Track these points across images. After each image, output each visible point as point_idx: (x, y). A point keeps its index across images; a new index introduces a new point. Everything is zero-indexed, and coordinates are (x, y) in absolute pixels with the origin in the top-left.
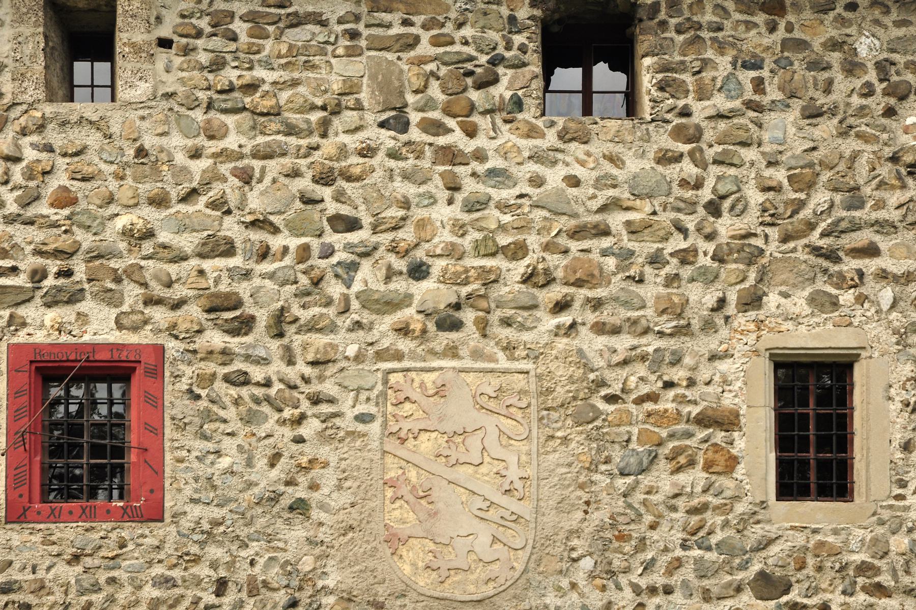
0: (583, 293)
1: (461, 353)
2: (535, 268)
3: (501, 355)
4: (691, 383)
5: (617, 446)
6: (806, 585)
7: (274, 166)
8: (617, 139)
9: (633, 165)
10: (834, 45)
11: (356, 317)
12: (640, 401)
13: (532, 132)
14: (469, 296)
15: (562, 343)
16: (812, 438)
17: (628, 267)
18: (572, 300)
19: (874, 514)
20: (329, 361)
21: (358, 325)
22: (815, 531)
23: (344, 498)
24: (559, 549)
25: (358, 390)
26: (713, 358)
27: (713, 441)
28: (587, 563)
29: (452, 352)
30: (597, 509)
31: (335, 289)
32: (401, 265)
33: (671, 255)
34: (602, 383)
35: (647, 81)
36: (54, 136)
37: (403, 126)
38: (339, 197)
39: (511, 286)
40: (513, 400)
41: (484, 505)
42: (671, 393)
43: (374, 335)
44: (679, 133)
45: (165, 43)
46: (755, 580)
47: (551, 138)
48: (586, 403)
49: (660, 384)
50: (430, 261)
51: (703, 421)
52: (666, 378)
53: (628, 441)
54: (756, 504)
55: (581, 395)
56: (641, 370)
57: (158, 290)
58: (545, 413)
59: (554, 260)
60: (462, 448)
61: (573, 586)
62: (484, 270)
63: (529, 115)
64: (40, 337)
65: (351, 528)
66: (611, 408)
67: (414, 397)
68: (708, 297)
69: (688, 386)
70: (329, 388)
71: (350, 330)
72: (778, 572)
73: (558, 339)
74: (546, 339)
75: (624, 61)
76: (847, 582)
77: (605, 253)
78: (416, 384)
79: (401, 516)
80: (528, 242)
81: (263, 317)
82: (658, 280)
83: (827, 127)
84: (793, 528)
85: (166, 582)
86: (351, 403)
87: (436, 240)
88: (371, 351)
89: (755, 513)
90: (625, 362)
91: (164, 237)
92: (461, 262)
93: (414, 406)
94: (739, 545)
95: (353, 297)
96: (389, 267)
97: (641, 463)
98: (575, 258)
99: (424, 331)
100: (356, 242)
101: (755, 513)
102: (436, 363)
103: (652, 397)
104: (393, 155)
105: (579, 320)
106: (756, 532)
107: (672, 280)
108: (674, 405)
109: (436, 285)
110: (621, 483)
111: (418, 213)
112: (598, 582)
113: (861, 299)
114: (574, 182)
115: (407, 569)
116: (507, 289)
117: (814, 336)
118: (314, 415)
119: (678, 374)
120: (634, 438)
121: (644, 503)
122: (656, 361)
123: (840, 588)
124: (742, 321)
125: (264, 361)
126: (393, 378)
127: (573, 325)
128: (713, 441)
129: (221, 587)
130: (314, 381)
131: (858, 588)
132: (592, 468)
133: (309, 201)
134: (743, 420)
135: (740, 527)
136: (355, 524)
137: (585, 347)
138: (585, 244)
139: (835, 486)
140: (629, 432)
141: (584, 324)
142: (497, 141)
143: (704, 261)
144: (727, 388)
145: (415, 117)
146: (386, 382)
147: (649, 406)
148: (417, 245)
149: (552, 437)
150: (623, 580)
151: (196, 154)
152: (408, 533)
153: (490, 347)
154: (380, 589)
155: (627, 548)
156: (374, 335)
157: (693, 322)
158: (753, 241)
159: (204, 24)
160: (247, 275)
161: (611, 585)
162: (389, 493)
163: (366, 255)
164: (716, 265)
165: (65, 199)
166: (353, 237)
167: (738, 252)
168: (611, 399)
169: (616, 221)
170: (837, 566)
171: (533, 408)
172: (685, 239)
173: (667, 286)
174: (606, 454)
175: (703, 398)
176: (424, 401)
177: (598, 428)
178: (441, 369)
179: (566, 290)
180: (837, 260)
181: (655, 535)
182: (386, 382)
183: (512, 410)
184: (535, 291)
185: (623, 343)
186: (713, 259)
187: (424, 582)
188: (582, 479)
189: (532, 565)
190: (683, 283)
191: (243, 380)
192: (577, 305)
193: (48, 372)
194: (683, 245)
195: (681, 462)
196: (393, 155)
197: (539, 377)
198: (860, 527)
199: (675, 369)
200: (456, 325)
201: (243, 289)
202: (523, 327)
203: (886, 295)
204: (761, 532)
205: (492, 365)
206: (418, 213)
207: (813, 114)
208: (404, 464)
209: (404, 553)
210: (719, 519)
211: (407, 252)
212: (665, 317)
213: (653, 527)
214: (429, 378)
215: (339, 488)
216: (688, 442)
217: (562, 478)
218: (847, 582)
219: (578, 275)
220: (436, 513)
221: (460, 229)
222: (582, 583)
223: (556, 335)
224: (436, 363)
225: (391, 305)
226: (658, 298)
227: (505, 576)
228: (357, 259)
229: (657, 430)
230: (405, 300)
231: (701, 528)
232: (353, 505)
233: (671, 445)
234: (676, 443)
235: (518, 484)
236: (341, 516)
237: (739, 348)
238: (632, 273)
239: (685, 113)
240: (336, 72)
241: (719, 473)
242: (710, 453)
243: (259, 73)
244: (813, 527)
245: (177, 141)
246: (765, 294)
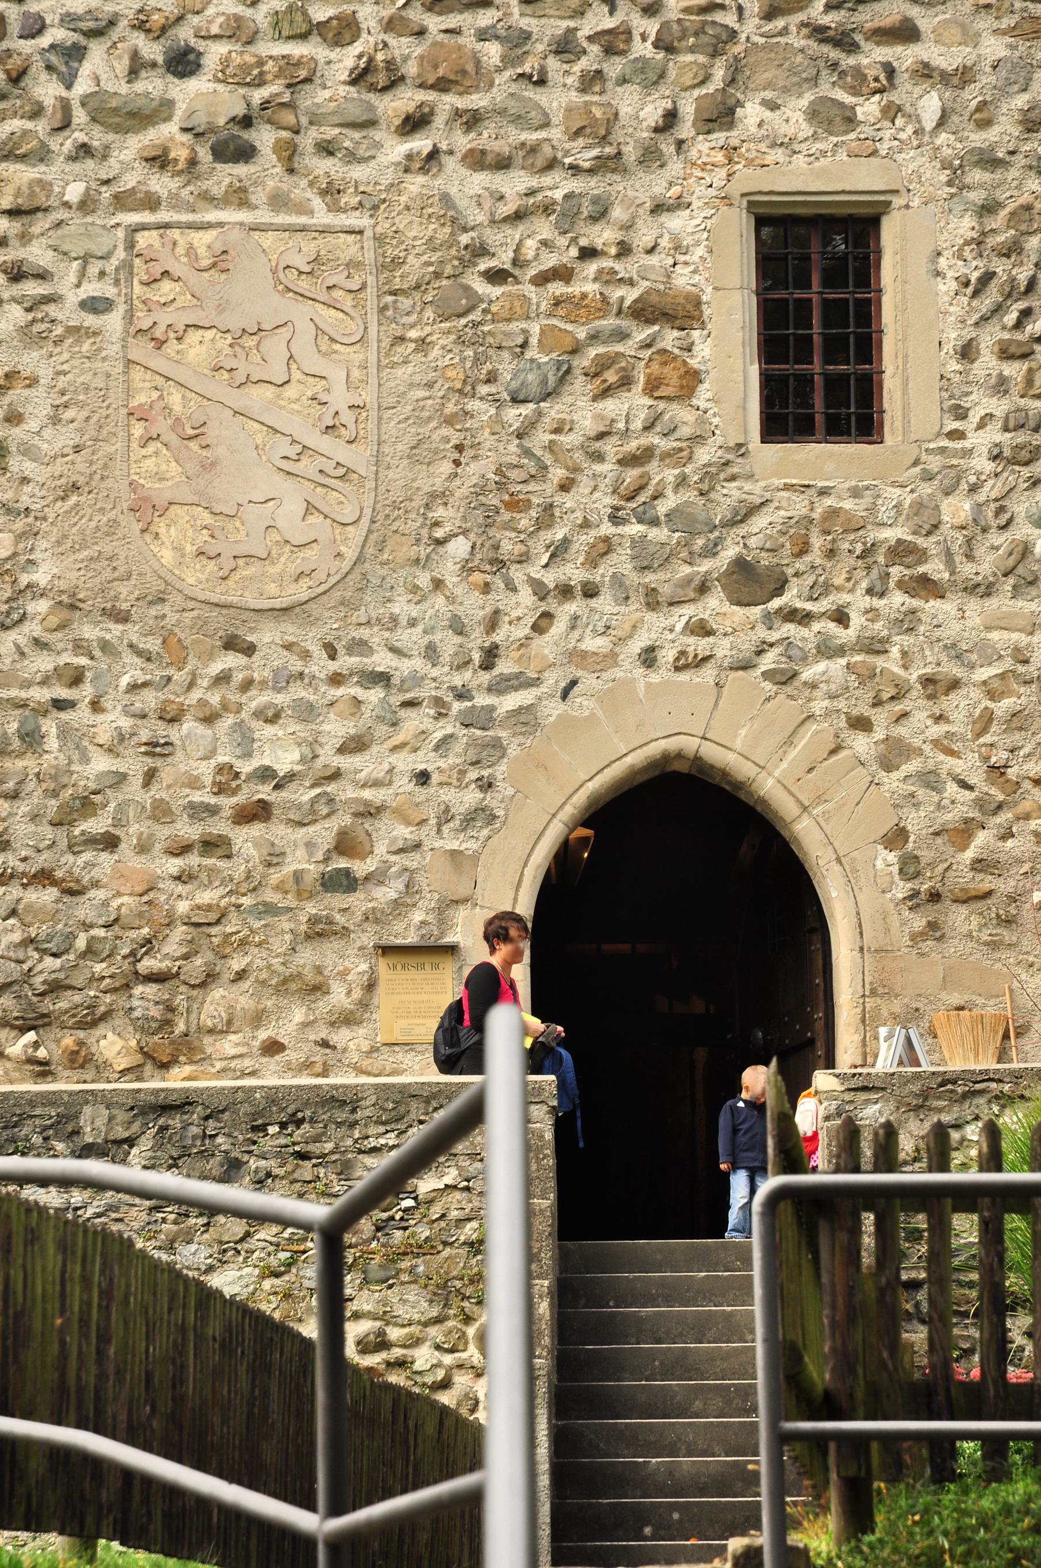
0: (450, 101)
1: (253, 199)
2: (371, 60)
3: (317, 203)
4: (624, 250)
5: (506, 355)
6: (810, 580)
11: (81, 137)
12: (542, 279)
14: (265, 105)
15: (415, 184)
16: (817, 340)
17: (520, 60)
18: (432, 113)
19: (916, 463)
20: (37, 210)
21: (84, 150)
22: (823, 492)
23: (63, 438)
24: (414, 524)
25: (86, 259)
26: (658, 208)
27: (660, 345)
28: (459, 547)
29: (239, 196)
30: (475, 457)
32: (153, 51)
33: (590, 39)
34: (481, 251)
40: (339, 278)
41: (292, 451)
42: (592, 268)
43: (111, 167)
46: (729, 573)
49: (574, 252)
50: (201, 45)
51: (644, 312)
52: (583, 242)
53: (524, 345)
54: (728, 449)
55: (448, 270)
56: (544, 228)
58: (389, 299)
59: (401, 46)
60: (255, 357)
61: (438, 584)
62: (289, 63)
65: (75, 487)
66: (496, 291)
67: (176, 270)
68: (649, 108)
69: (618, 256)
70: (38, 254)
71: (73, 158)
72: (766, 560)
73: (409, 177)
74: (389, 177)
76: (875, 573)
77: (483, 35)
78: (180, 250)
79: (157, 468)
80: (360, 16)
82: (569, 80)
84: (788, 487)
86: (73, 279)
87: (211, 11)
88: (106, 193)
89: (727, 463)
90: (518, 216)
92: (251, 49)
93: (177, 287)
94: (702, 516)
95: (75, 104)
96: (135, 55)
97: (544, 382)
98: (435, 44)
99: (193, 162)
100: (80, 11)
101: (727, 463)
102: (212, 216)
103: (562, 274)
105: (444, 146)
106: (729, 495)
108: (596, 286)
109: (211, 85)
110: (515, 415)
112: (478, 577)
113: (891, 112)
115: (167, 556)
116: (327, 94)
117: (820, 174)
118: (14, 300)
119: (603, 236)
120: (534, 341)
121: (551, 447)
122: (568, 214)
123: (864, 585)
124: (703, 148)
126: (143, 239)
127: (434, 155)
128: (660, 345)
130: (13, 242)
131: (892, 585)
132: (466, 390)
134: (707, 311)
135: (705, 487)
136: (81, 481)
137: (453, 191)
138: (452, 21)
139: (853, 418)
140: (524, 331)
141: (451, 153)
143: (641, 49)
144: (681, 258)
146: (130, 245)
147: (557, 288)
148: (180, 19)
149: (402, 339)
150: (517, 574)
152: (168, 496)
153: (300, 189)
154: (123, 589)
155: (524, 522)
156: (111, 167)
157: (626, 149)
158: (719, 17)
161: (499, 582)
162: (138, 430)
163: (97, 33)
164: (661, 55)
167: (696, 34)
168: (497, 276)
170: (859, 548)
171: (371, 292)
172: (611, 13)
173: (583, 91)
174: (488, 366)
176: (193, 278)
177: (475, 325)
178: (221, 224)
179: (422, 96)
180: (853, 48)
181: (568, 501)
182: (130, 245)
183: (337, 294)
184: (372, 97)
185: (514, 184)
186: (656, 45)
187: (195, 577)
188: (450, 408)
189: (370, 550)
190: (609, 85)
192: (439, 120)
194: (609, 23)
197: (379, 240)
198: (893, 484)
199: (597, 227)
200: (245, 153)
202: (352, 157)
204: (736, 494)
205: (303, 220)
208: (160, 381)
209: (162, 530)
210: (671, 474)
211: (164, 30)
212: (581, 142)
213: (565, 487)
214: (202, 239)
215: (55, 420)
216: (619, 348)
217: (419, 405)
218: (875, 573)
219: (441, 72)
220: (213, 464)
222: (451, 580)
223: (407, 170)
224: (212, 216)
226: (569, 110)
227: (327, 568)
228: (83, 41)
229: (569, 327)
230: (163, 110)
231: (642, 488)
232: (77, 449)
233: (592, 352)
234: (601, 350)
235: (347, 417)
236: (58, 467)
237: (699, 194)
238: (527, 68)
241: (669, 399)
242: (655, 366)
244: (820, 484)
246: (739, 104)
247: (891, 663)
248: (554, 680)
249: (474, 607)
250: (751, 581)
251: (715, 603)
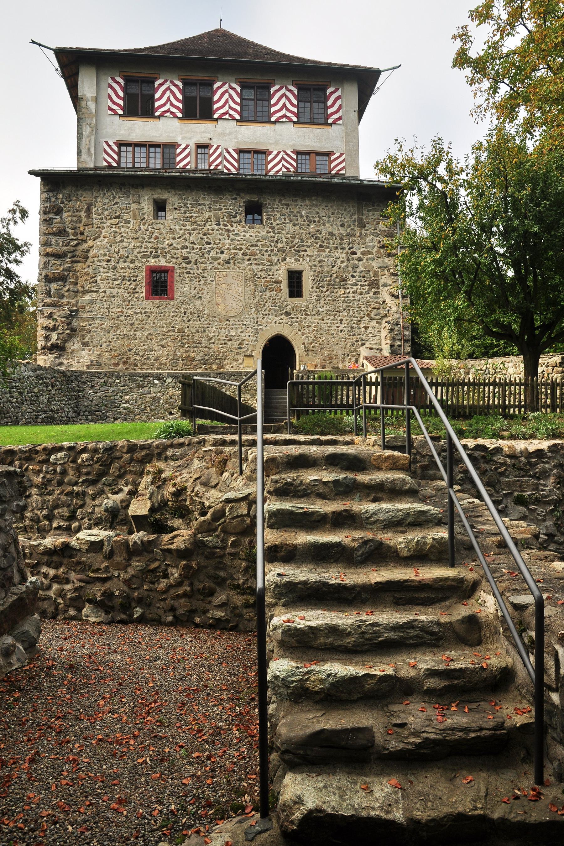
7: (195, 232)
8: (259, 228)
9: (262, 233)
10: (298, 212)
13: (243, 227)
15: (249, 267)
23: (208, 296)
28: (254, 309)
29: (229, 268)
31: (207, 256)
32: (219, 251)
35: (264, 218)
36: (155, 226)
37: (219, 225)
38: (207, 238)
39: (239, 256)
44: (270, 228)
45: (175, 209)
47: (247, 228)
48: (253, 278)
51: (275, 282)
56: (264, 272)
57: (173, 256)
59: (247, 251)
63: (243, 223)
64: (151, 264)
70: (205, 275)
75: (260, 214)
79: (219, 300)
81: (193, 261)
83: (297, 227)
85: (174, 312)
91: (174, 245)
103: (266, 278)
104: (218, 230)
106: (285, 304)
107: (269, 255)
110: (260, 294)
111: (222, 242)
113: (304, 260)
114: (251, 236)
117: (295, 266)
119: (271, 273)
122: (267, 271)
124: (282, 263)
125: (193, 269)
129: (185, 313)
133: (202, 239)
142: (237, 228)
145: (221, 223)
151: (181, 230)
153: (236, 267)
159: (183, 205)
160: (190, 253)
165: (156, 238)
166: (210, 246)
168: (258, 278)
169: (259, 244)
175: (275, 278)
185: (260, 267)
187: (223, 312)
191: (189, 273)
193: (153, 271)
195: (271, 290)
196: (218, 230)
200: (229, 263)
201: (189, 256)
203: (308, 259)
206: (222, 242)
207: (295, 225)
221: (230, 245)
225: (217, 259)
227: (239, 312)
239: (272, 224)
240: (207, 214)
243: (193, 214)
247: (303, 323)
248: (264, 325)
249: (255, 316)
250: (287, 314)
251: (283, 316)
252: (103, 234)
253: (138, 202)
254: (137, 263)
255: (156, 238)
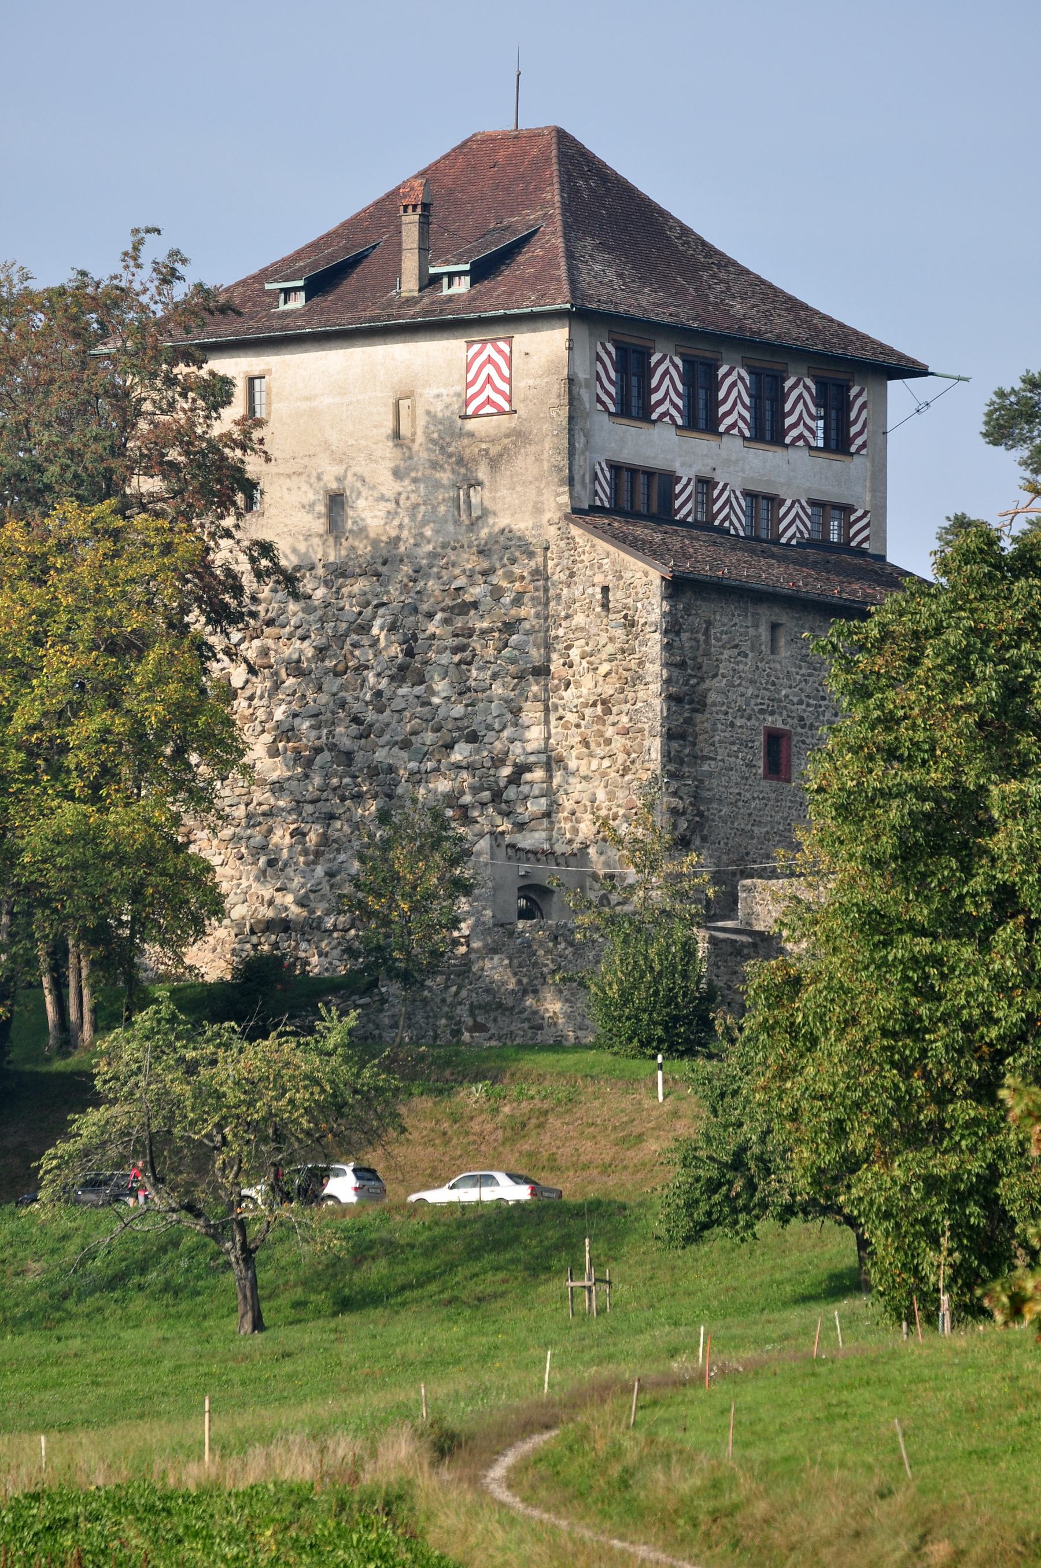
7: (811, 679)
201: (805, 715)
245: (794, 670)
252: (721, 671)
253: (756, 626)
254: (753, 721)
255: (773, 684)
